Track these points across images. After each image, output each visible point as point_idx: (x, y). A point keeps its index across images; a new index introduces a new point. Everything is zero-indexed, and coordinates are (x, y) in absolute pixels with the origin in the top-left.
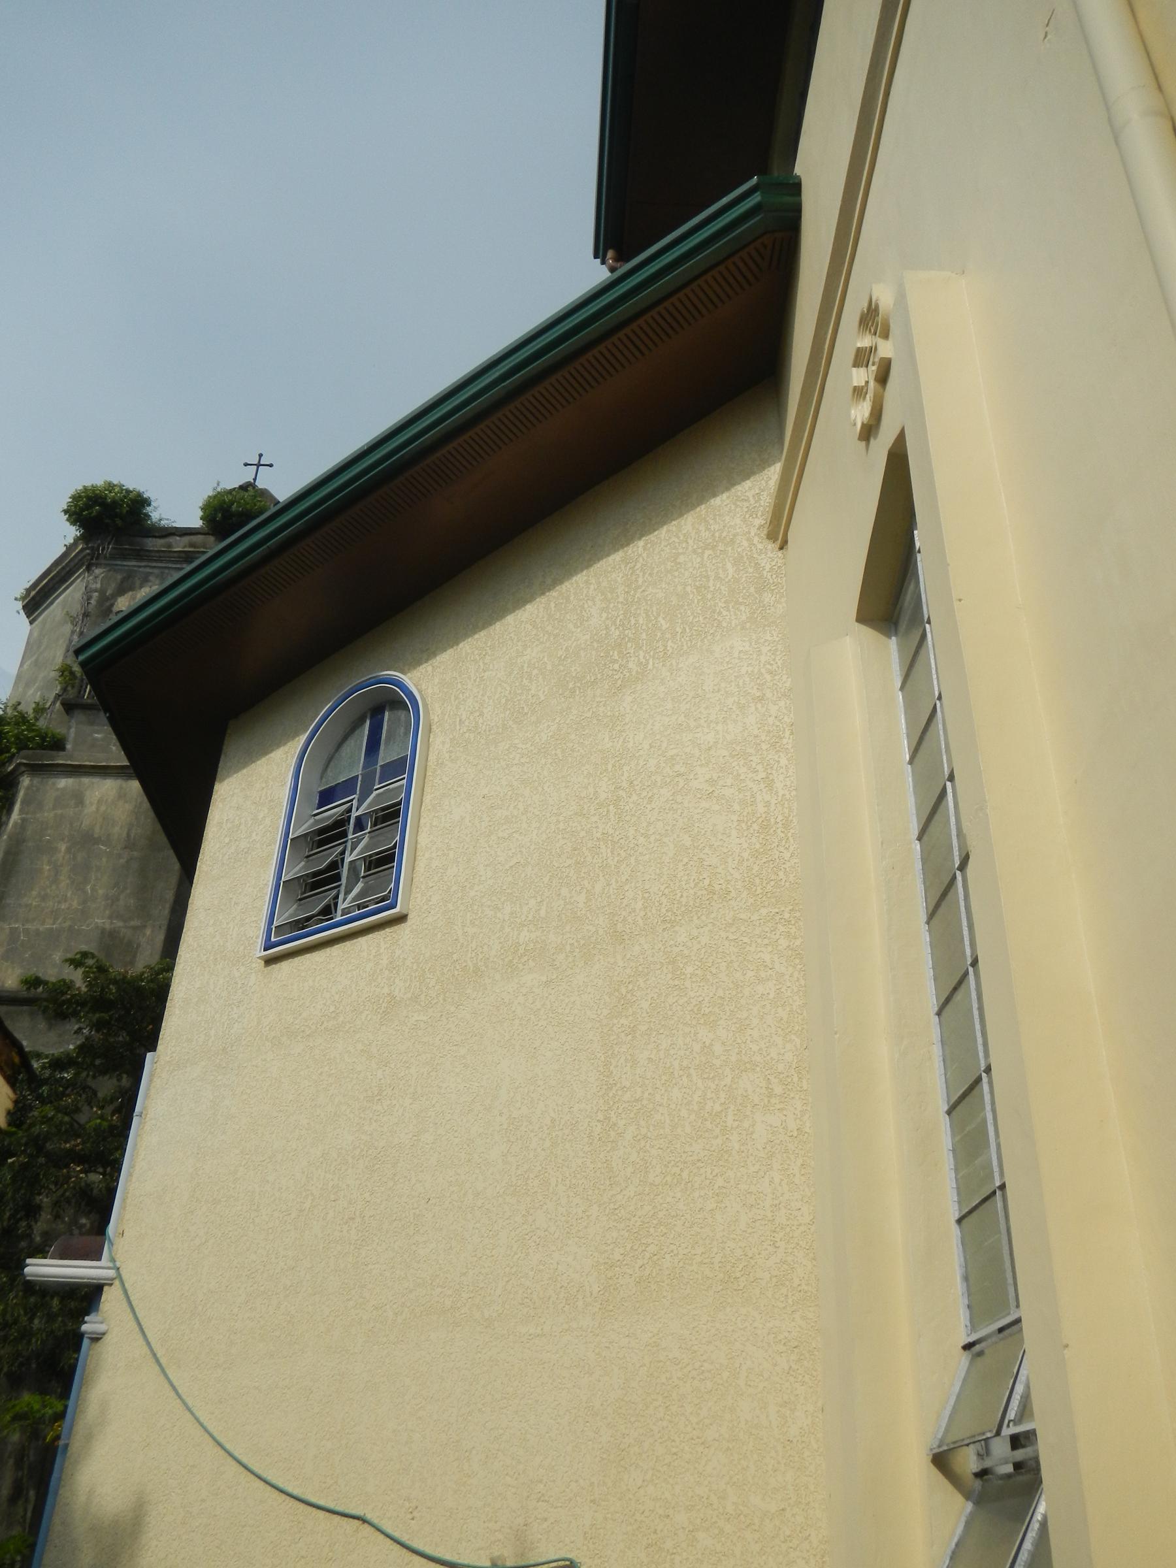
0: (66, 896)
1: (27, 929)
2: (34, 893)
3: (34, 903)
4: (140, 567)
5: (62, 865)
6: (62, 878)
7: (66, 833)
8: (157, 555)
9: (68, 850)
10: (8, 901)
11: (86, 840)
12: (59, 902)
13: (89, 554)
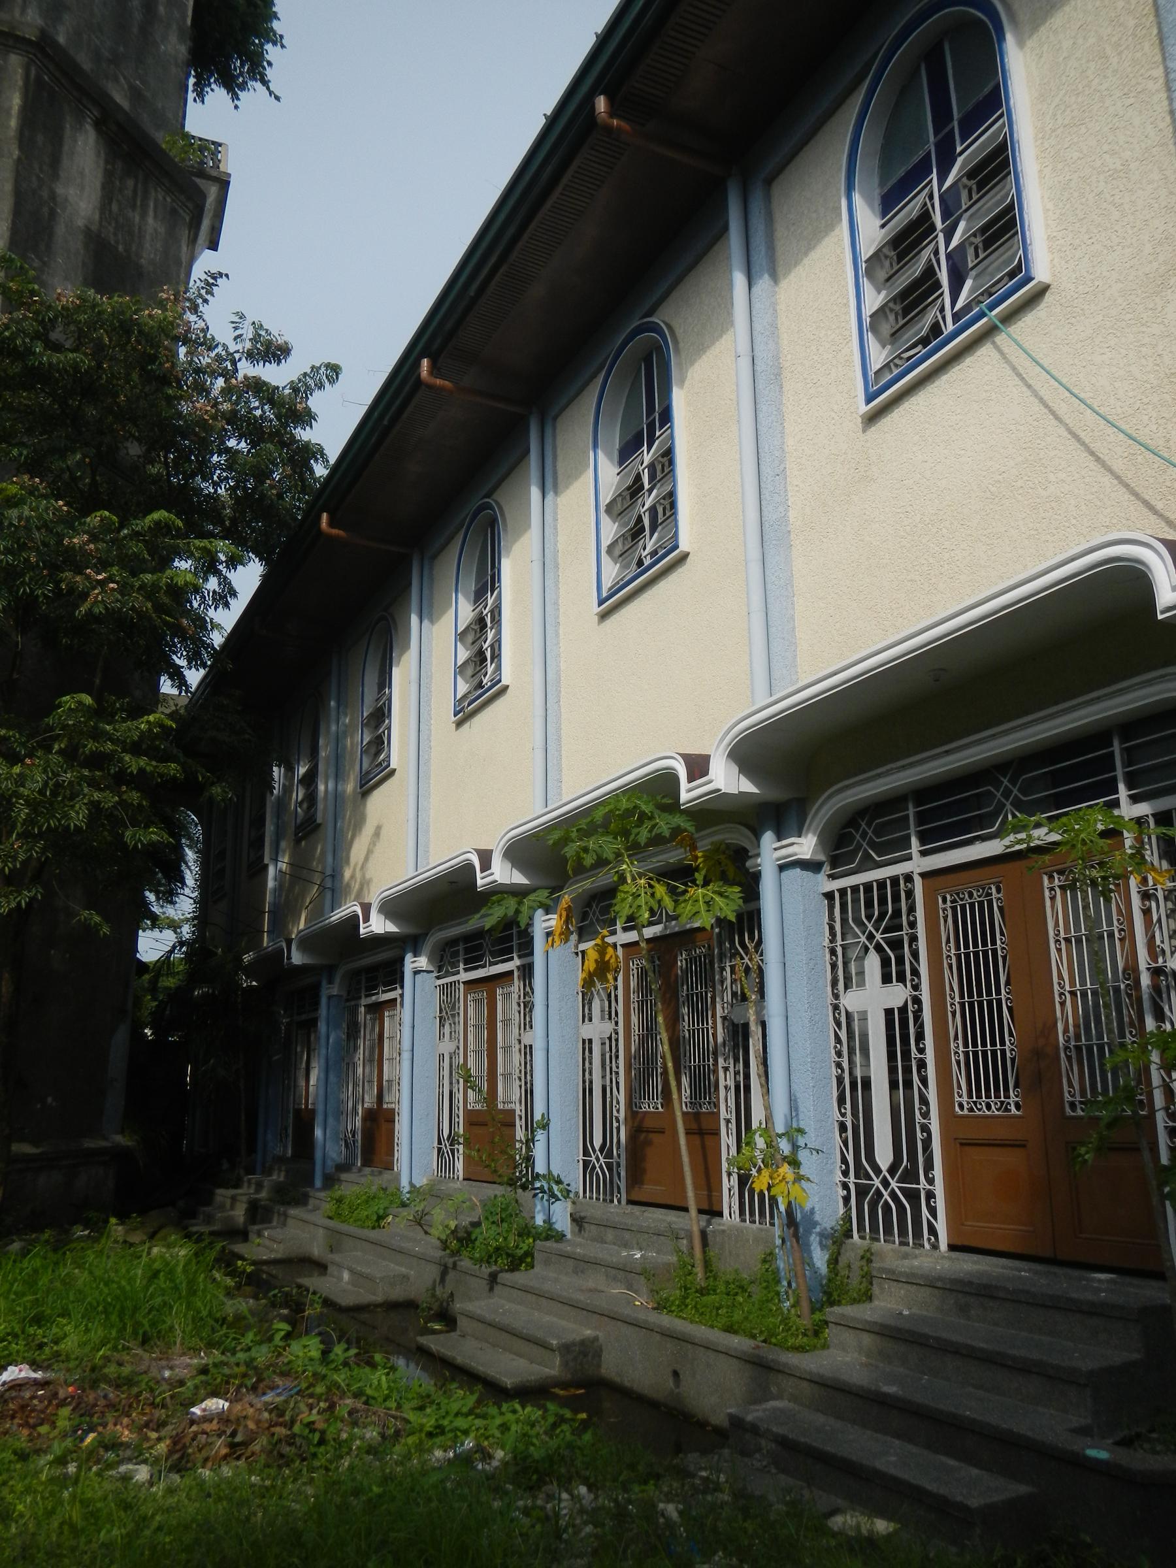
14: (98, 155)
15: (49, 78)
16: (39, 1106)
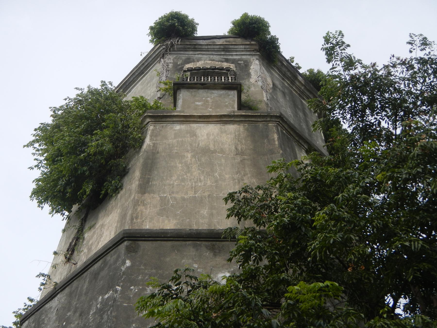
0: (200, 179)
1: (175, 198)
4: (195, 54)
7: (189, 148)
8: (206, 47)
9: (193, 156)
11: (206, 151)
13: (164, 49)
15: (286, 132)
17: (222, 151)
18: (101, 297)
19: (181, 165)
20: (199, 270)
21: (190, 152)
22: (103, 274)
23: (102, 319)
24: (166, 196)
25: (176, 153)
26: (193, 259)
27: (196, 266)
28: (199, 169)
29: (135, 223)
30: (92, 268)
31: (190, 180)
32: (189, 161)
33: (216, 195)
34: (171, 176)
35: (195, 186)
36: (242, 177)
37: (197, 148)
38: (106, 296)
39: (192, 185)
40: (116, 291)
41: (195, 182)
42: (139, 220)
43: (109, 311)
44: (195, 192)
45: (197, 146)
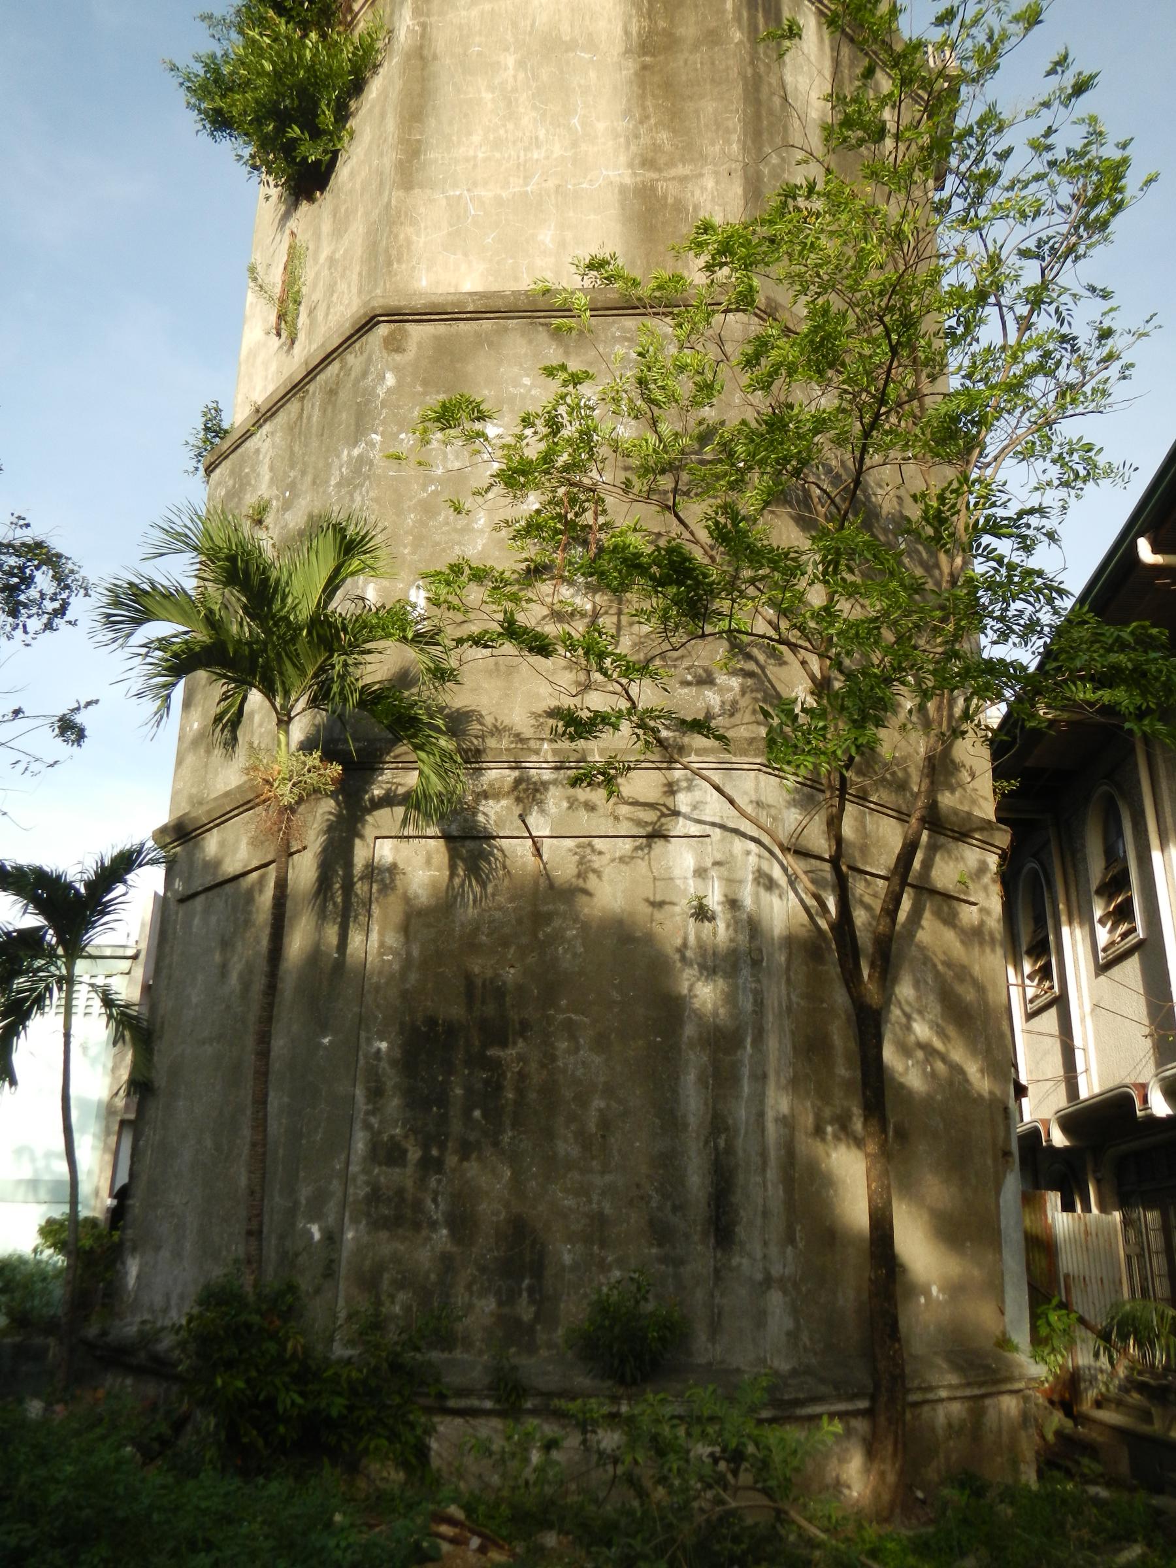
0: (537, 138)
2: (476, 139)
3: (480, 155)
5: (515, 90)
6: (522, 110)
7: (510, 37)
9: (521, 64)
10: (431, 155)
12: (526, 149)
14: (821, 40)
16: (922, 1300)
17: (591, 44)
18: (346, 452)
19: (490, 96)
20: (533, 392)
21: (512, 49)
22: (343, 396)
23: (352, 500)
24: (460, 197)
25: (480, 54)
26: (521, 365)
27: (527, 381)
28: (534, 107)
29: (396, 275)
30: (321, 378)
31: (514, 143)
32: (511, 80)
33: (575, 185)
34: (469, 134)
35: (526, 161)
36: (636, 127)
37: (530, 34)
38: (356, 452)
39: (518, 158)
40: (372, 444)
41: (526, 149)
42: (404, 266)
43: (362, 486)
44: (525, 178)
45: (529, 29)
